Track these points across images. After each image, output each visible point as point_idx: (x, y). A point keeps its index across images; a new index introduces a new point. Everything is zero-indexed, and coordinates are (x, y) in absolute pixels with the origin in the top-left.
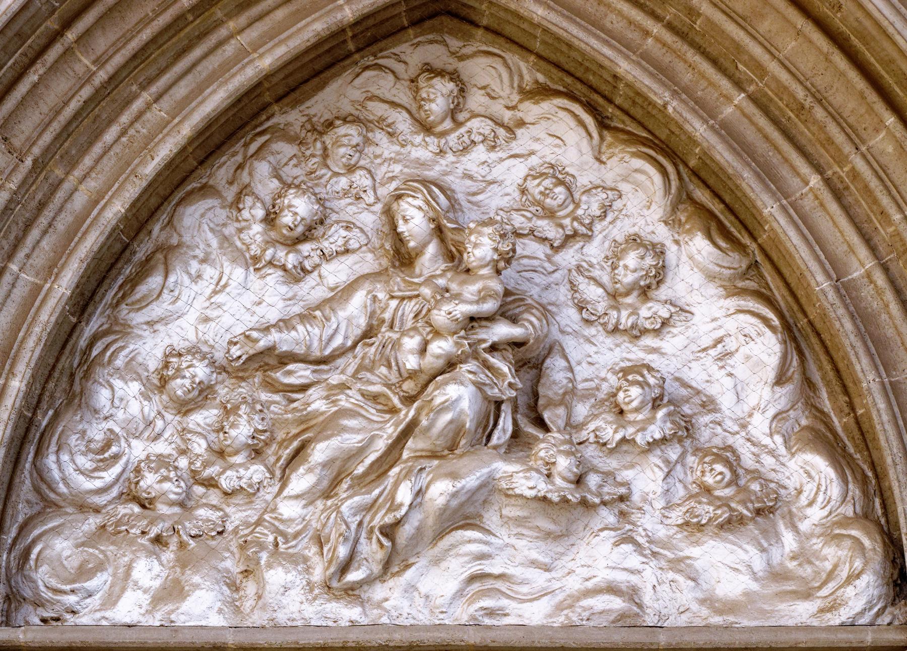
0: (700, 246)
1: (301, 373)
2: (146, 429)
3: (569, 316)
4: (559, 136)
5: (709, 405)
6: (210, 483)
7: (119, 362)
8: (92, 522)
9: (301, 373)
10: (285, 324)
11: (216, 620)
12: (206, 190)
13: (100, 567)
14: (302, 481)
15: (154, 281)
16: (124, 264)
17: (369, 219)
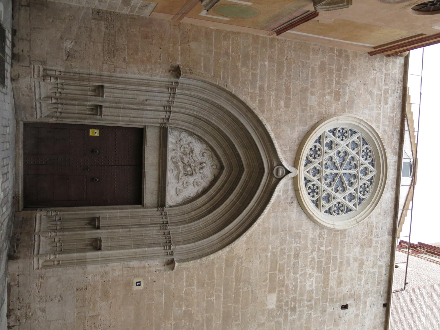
0: (201, 190)
1: (191, 155)
2: (186, 141)
3: (195, 178)
4: (210, 177)
5: (187, 190)
8: (178, 136)
9: (191, 155)
10: (195, 153)
12: (207, 147)
14: (181, 154)
15: (199, 142)
16: (200, 139)
17: (204, 161)
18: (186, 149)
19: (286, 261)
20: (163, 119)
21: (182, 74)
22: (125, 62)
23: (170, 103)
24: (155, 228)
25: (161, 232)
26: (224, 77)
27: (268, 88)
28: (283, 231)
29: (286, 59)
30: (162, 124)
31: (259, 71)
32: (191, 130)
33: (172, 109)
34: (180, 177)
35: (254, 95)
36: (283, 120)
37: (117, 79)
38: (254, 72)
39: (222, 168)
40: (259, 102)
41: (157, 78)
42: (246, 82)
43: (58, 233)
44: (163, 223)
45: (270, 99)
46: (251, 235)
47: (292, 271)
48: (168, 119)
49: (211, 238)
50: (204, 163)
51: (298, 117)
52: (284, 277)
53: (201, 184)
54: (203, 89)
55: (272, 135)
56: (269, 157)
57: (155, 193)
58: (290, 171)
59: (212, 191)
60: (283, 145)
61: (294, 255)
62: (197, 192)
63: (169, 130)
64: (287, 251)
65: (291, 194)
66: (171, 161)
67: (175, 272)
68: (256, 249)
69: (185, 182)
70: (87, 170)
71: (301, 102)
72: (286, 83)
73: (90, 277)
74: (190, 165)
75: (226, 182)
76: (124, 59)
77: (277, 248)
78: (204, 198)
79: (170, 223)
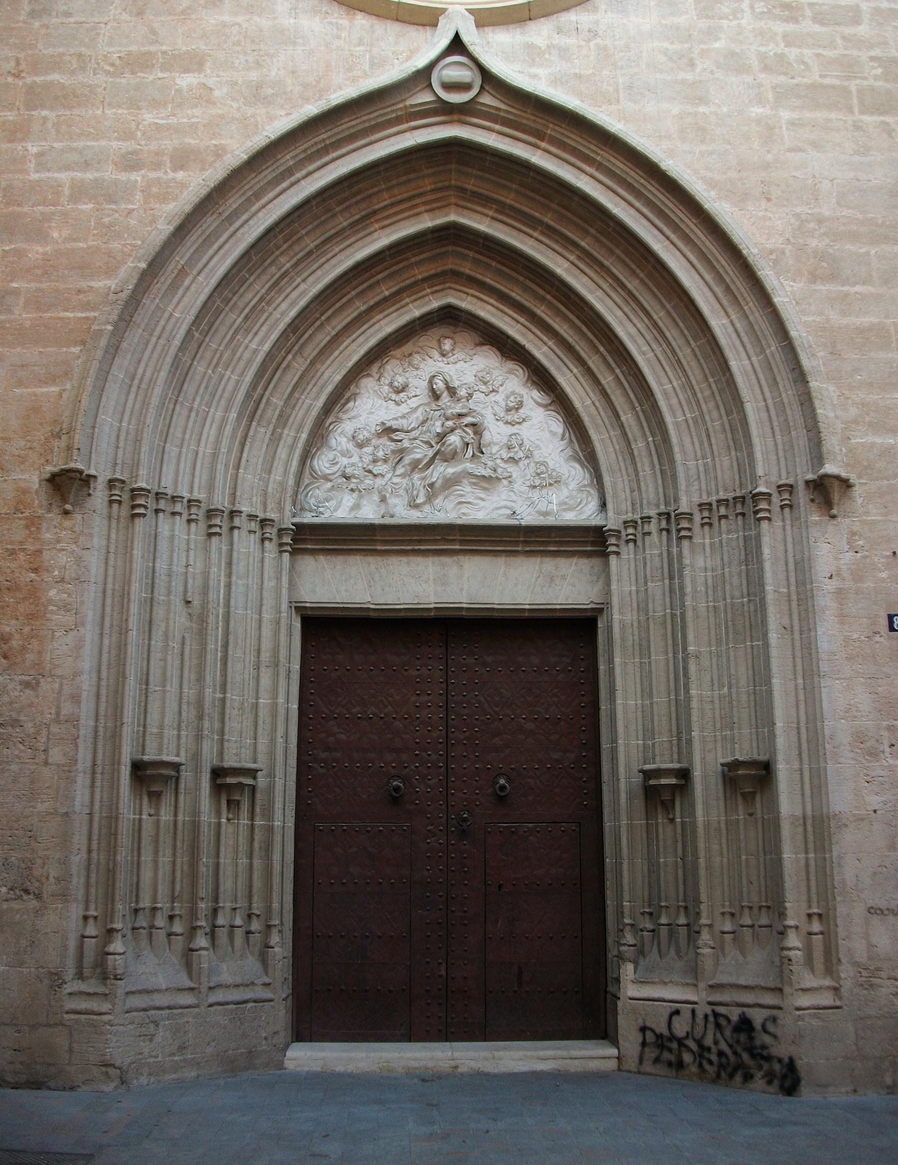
0: (536, 394)
2: (346, 454)
6: (370, 472)
7: (339, 431)
8: (329, 485)
10: (396, 419)
11: (371, 516)
12: (369, 375)
13: (332, 499)
14: (400, 470)
15: (351, 404)
18: (380, 454)
19: (808, 52)
20: (263, 540)
21: (72, 465)
22: (38, 683)
23: (199, 513)
24: (687, 561)
25: (703, 537)
26: (87, 306)
27: (128, 135)
28: (692, 64)
29: (17, 76)
30: (281, 545)
31: (63, 176)
32: (304, 436)
33: (221, 501)
34: (487, 472)
35: (155, 190)
36: (254, 75)
37: (102, 711)
38: (67, 192)
39: (450, 318)
40: (182, 168)
41: (94, 562)
42: (106, 220)
43: (704, 921)
44: (668, 531)
45: (169, 127)
46: (712, 184)
47: (848, 31)
48: (264, 522)
49: (723, 341)
50: (431, 382)
51: (239, 19)
52: (872, 59)
53: (513, 393)
54: (136, 382)
55: (312, 109)
56: (398, 121)
57: (549, 565)
58: (451, 35)
59: (541, 350)
60: (350, 70)
61: (787, 20)
62: (545, 406)
63: (308, 518)
64: (771, 49)
65: (545, 32)
66: (427, 508)
67: (860, 476)
68: (766, 166)
69: (505, 455)
70: (465, 820)
71: (183, 12)
72: (108, 73)
73: (874, 801)
74: (441, 437)
75: (504, 298)
76: (27, 685)
77: (760, 85)
78: (568, 380)
79: (667, 504)
